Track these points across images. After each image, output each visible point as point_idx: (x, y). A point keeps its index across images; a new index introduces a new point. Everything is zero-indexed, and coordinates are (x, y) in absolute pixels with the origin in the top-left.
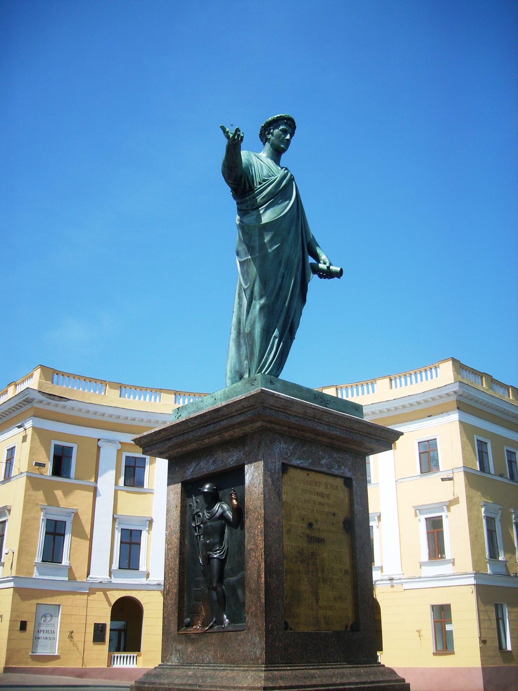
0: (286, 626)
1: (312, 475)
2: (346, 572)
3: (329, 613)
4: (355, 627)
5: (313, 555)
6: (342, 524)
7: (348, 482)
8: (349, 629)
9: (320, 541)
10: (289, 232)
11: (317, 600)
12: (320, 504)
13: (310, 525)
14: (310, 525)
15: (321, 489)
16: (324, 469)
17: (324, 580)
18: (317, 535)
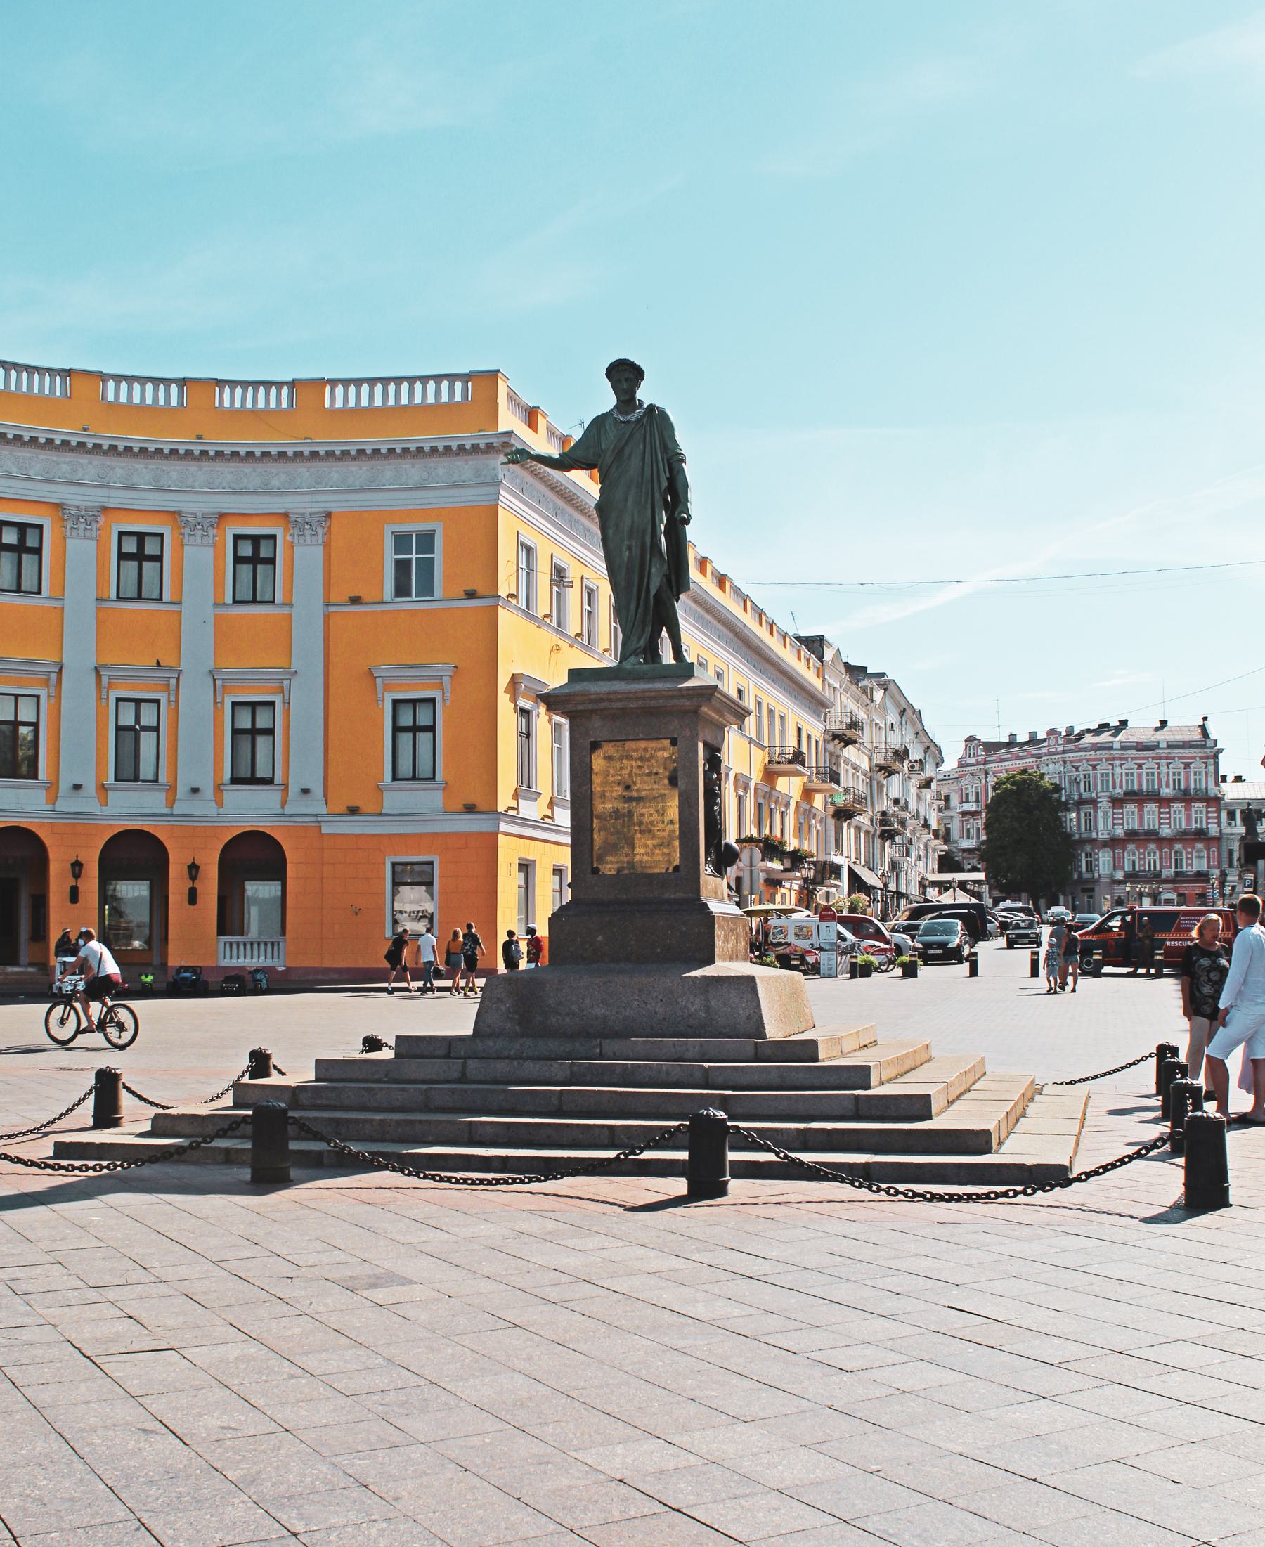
0: (596, 871)
1: (629, 745)
2: (671, 822)
3: (645, 858)
4: (676, 869)
5: (630, 813)
6: (666, 781)
7: (674, 742)
8: (671, 870)
9: (639, 800)
10: (626, 500)
11: (633, 849)
12: (639, 767)
13: (628, 788)
14: (628, 788)
15: (641, 753)
16: (641, 736)
17: (641, 832)
18: (635, 794)
